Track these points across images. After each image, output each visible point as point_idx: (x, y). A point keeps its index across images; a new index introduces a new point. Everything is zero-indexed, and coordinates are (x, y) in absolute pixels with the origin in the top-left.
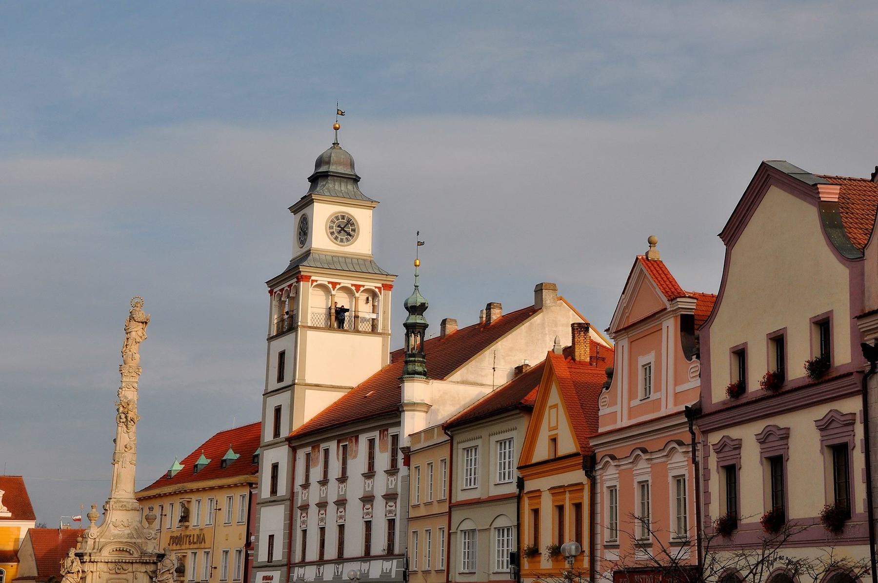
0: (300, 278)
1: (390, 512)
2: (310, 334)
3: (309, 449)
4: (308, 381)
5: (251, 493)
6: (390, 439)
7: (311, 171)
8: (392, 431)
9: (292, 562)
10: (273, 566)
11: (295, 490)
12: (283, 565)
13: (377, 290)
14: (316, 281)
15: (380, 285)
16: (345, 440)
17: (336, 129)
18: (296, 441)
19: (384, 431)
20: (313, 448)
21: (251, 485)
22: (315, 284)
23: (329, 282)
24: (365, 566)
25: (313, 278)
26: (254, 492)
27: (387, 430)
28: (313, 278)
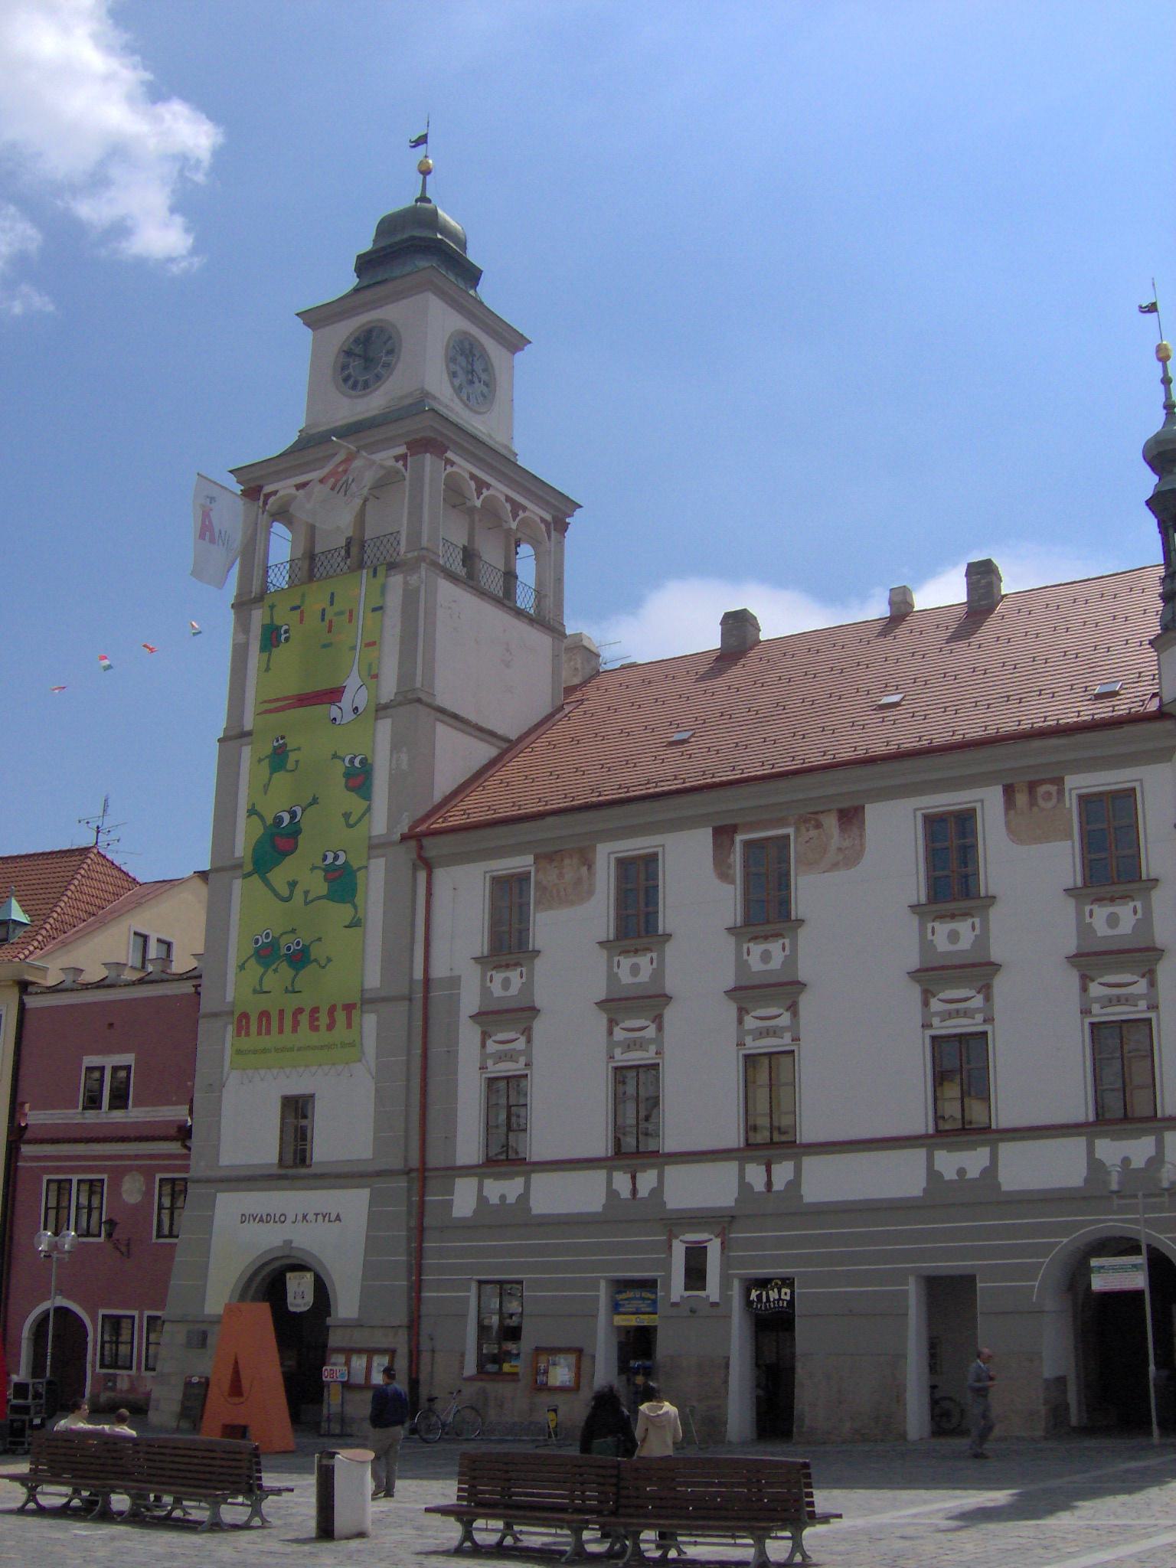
0: (421, 445)
1: (1119, 1000)
2: (446, 589)
3: (523, 862)
4: (440, 701)
5: (22, 1008)
6: (1071, 803)
7: (366, 245)
8: (1079, 783)
9: (433, 1161)
10: (316, 1176)
11: (439, 971)
12: (379, 1174)
13: (543, 526)
14: (452, 464)
15: (548, 517)
16: (782, 822)
17: (425, 172)
18: (425, 843)
19: (1032, 787)
20: (547, 857)
21: (24, 986)
22: (449, 469)
23: (473, 477)
24: (963, 1162)
25: (449, 455)
26: (32, 1002)
27: (1059, 781)
28: (449, 455)
